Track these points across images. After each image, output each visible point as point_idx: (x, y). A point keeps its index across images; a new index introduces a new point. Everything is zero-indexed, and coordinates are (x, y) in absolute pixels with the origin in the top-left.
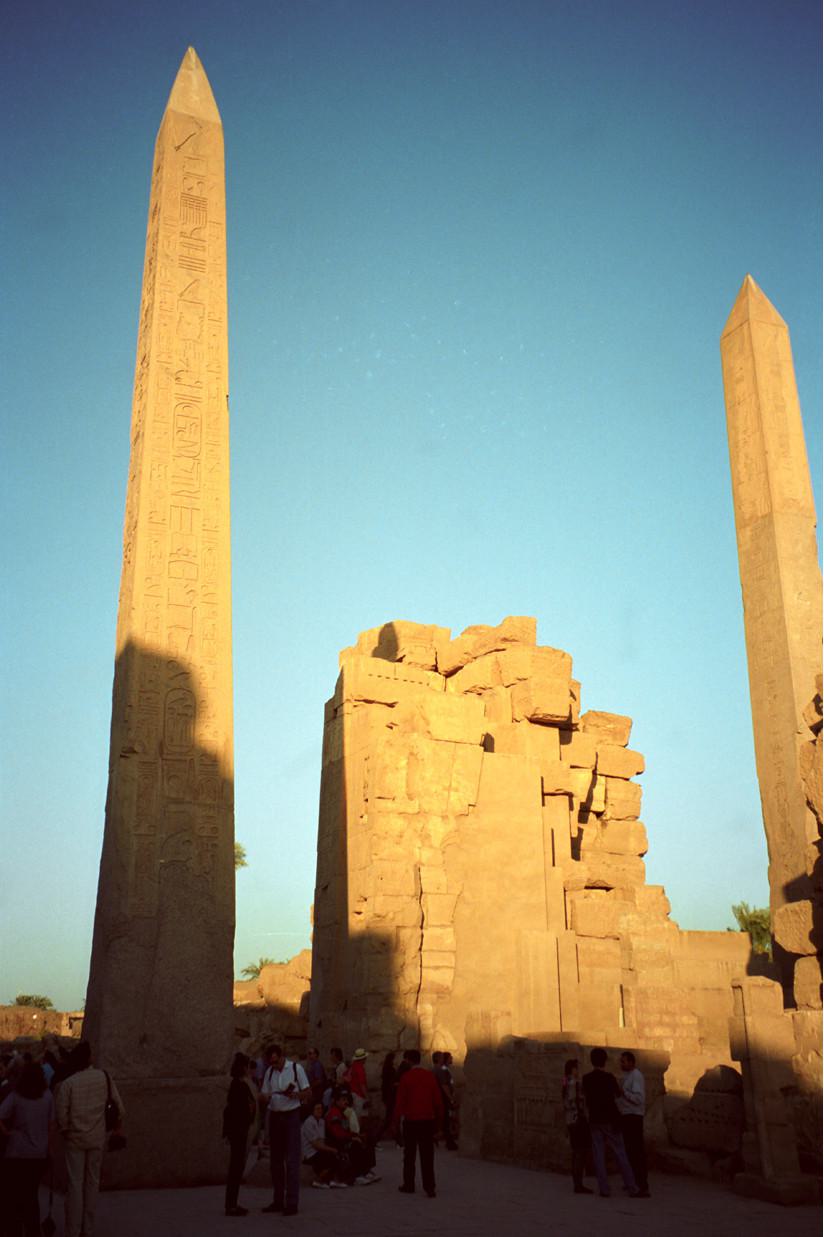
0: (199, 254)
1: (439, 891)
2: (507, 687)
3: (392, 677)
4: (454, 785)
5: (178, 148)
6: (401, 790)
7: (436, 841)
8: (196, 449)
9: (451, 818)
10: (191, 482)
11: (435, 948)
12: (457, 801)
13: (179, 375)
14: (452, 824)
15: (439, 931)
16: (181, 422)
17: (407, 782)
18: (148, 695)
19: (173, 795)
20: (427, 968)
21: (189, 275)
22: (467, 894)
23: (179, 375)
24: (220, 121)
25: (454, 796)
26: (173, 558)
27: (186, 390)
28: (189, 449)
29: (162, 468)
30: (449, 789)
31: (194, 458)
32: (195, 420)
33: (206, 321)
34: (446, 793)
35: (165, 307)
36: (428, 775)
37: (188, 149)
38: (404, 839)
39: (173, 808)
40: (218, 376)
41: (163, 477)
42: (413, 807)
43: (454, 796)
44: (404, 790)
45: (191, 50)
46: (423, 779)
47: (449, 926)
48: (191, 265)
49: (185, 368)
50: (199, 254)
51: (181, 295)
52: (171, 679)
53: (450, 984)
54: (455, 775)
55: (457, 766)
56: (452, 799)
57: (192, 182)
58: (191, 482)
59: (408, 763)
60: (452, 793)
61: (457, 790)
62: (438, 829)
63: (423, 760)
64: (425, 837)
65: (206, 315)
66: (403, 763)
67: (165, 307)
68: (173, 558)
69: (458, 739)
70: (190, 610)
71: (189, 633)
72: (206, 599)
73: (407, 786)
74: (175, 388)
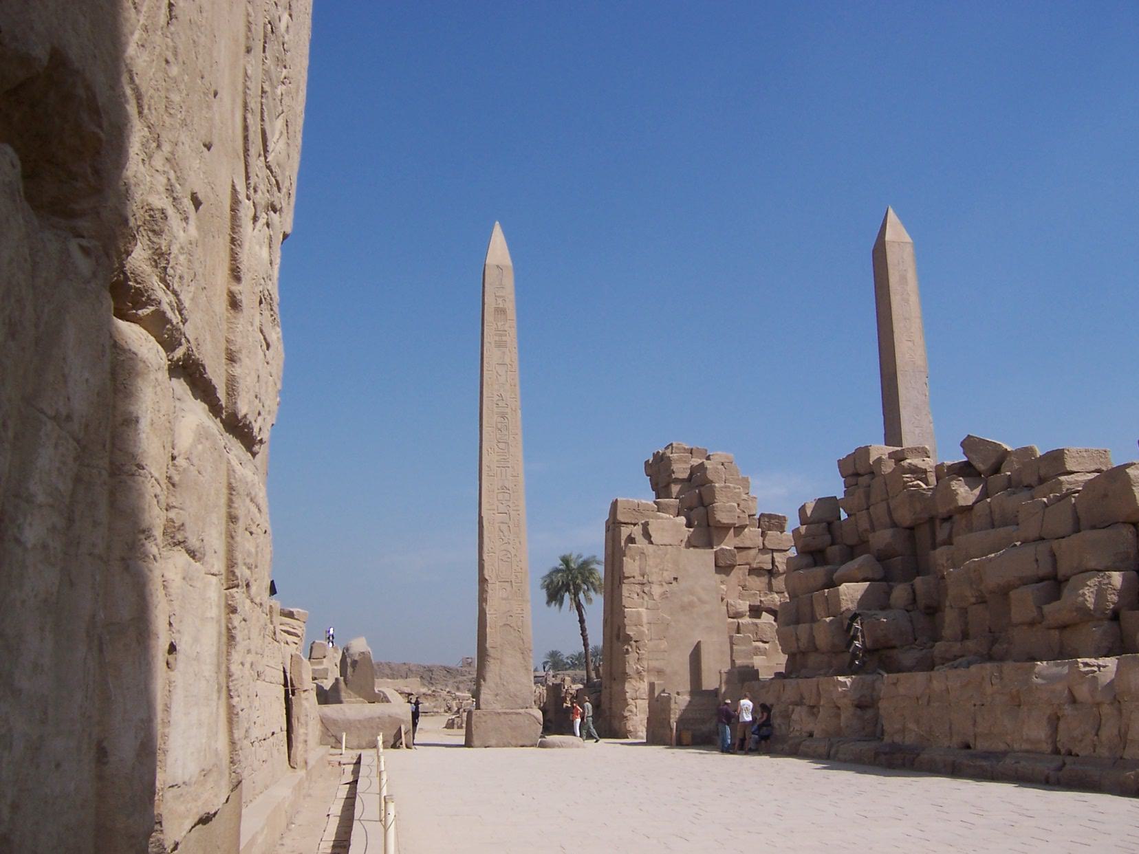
0: (504, 338)
3: (637, 509)
4: (665, 568)
6: (637, 574)
9: (664, 583)
12: (668, 576)
17: (640, 568)
22: (673, 623)
23: (498, 403)
24: (511, 264)
30: (662, 570)
31: (506, 443)
34: (661, 572)
39: (504, 601)
43: (665, 574)
44: (638, 572)
45: (497, 223)
48: (501, 345)
50: (504, 338)
55: (668, 556)
56: (664, 575)
59: (640, 559)
60: (664, 572)
61: (667, 570)
66: (637, 558)
72: (515, 508)
74: (496, 410)
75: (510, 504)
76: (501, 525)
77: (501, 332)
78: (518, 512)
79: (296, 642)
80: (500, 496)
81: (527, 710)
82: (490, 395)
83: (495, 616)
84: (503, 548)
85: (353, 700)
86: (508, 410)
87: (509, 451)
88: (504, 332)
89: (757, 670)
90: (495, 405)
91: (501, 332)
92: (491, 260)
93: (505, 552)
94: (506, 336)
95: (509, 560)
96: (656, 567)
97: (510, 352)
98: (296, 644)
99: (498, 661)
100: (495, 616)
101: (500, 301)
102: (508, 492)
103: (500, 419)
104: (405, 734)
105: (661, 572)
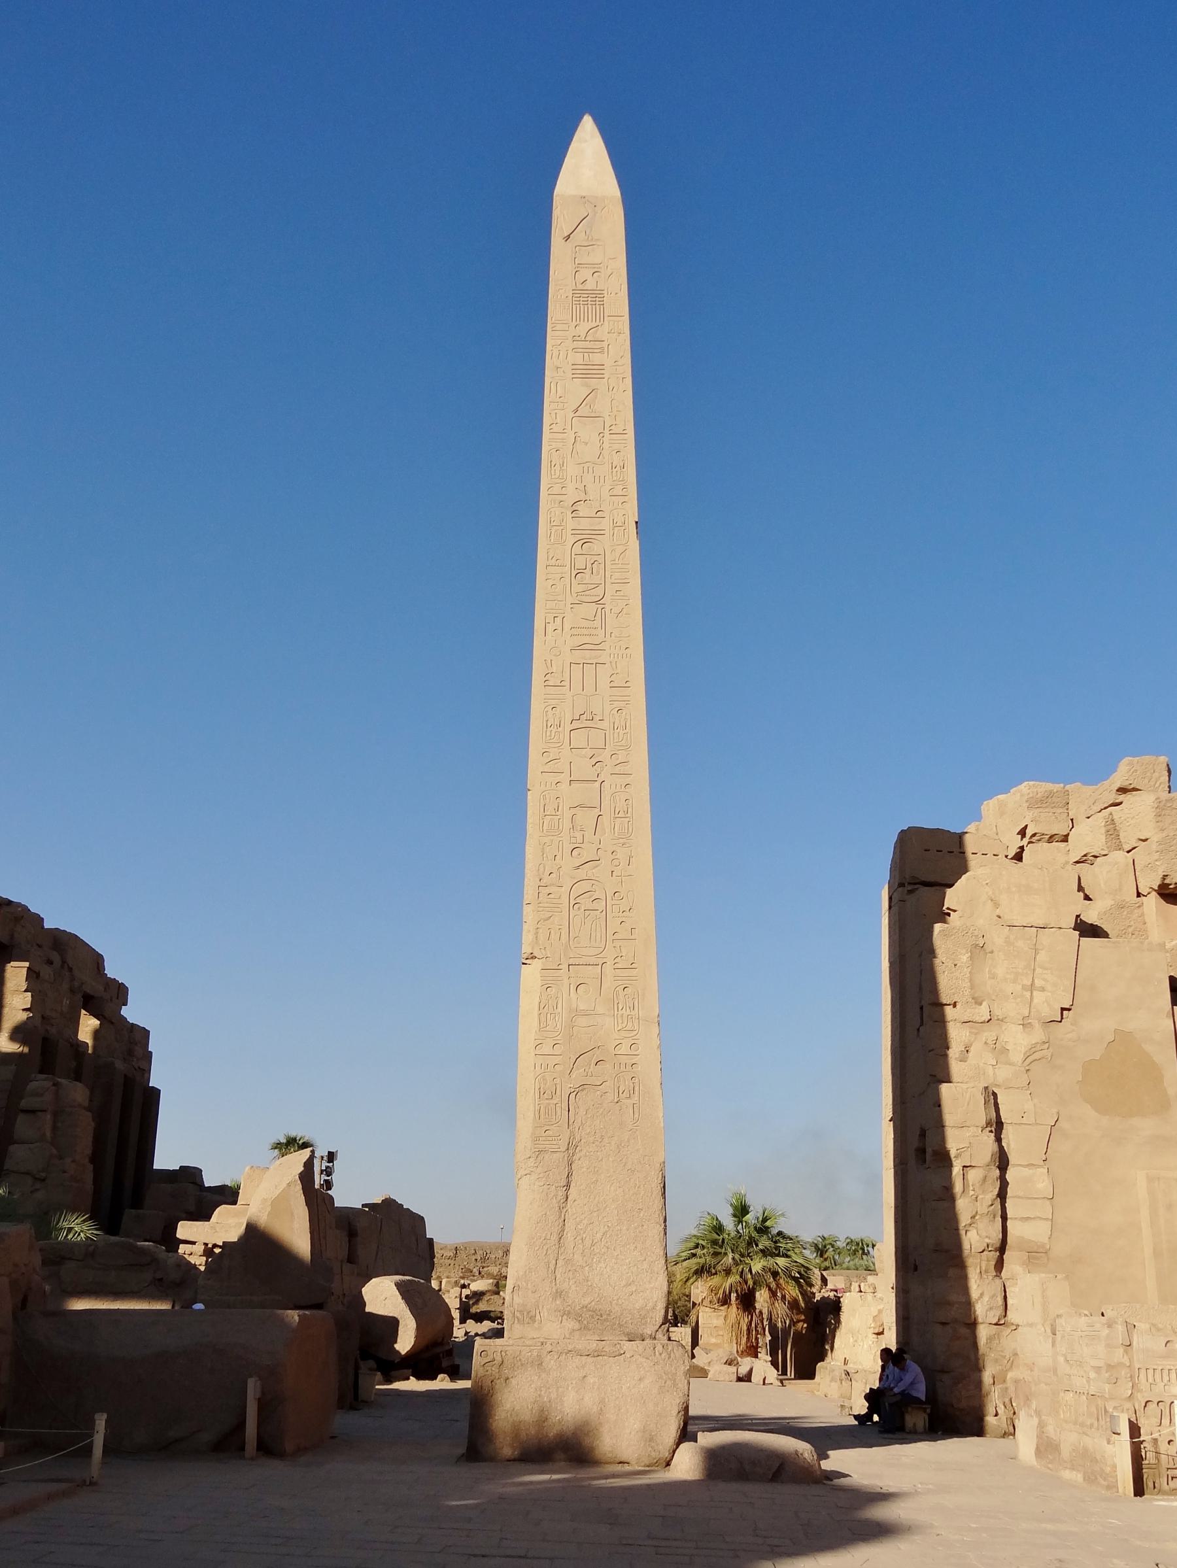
0: (597, 358)
1: (1024, 1121)
2: (1128, 852)
4: (1038, 983)
7: (1017, 1057)
8: (599, 591)
9: (1037, 1025)
10: (593, 632)
11: (1021, 1194)
12: (1046, 1004)
13: (574, 508)
14: (1038, 1034)
15: (1027, 1172)
17: (971, 980)
19: (582, 1007)
20: (1047, 1219)
25: (1039, 997)
26: (576, 725)
27: (584, 524)
29: (558, 620)
32: (596, 558)
35: (556, 428)
36: (1000, 971)
37: (579, 236)
38: (970, 1054)
40: (622, 499)
41: (559, 631)
42: (982, 1013)
46: (993, 977)
47: (1040, 1166)
49: (583, 497)
52: (578, 868)
53: (1046, 1240)
54: (1038, 970)
55: (1042, 956)
56: (1035, 1001)
57: (585, 273)
58: (593, 632)
59: (971, 958)
60: (1035, 993)
61: (1043, 989)
62: (1018, 1040)
63: (992, 952)
64: (999, 1050)
65: (607, 431)
66: (965, 958)
67: (556, 428)
68: (576, 725)
69: (1041, 923)
70: (597, 784)
71: (596, 812)
72: (617, 770)
73: (972, 987)
74: (570, 524)
75: (605, 756)
78: (628, 780)
80: (579, 738)
82: (556, 489)
84: (581, 874)
86: (605, 524)
87: (604, 624)
90: (570, 515)
92: (566, 186)
94: (602, 352)
95: (595, 905)
96: (1015, 981)
105: (1028, 994)
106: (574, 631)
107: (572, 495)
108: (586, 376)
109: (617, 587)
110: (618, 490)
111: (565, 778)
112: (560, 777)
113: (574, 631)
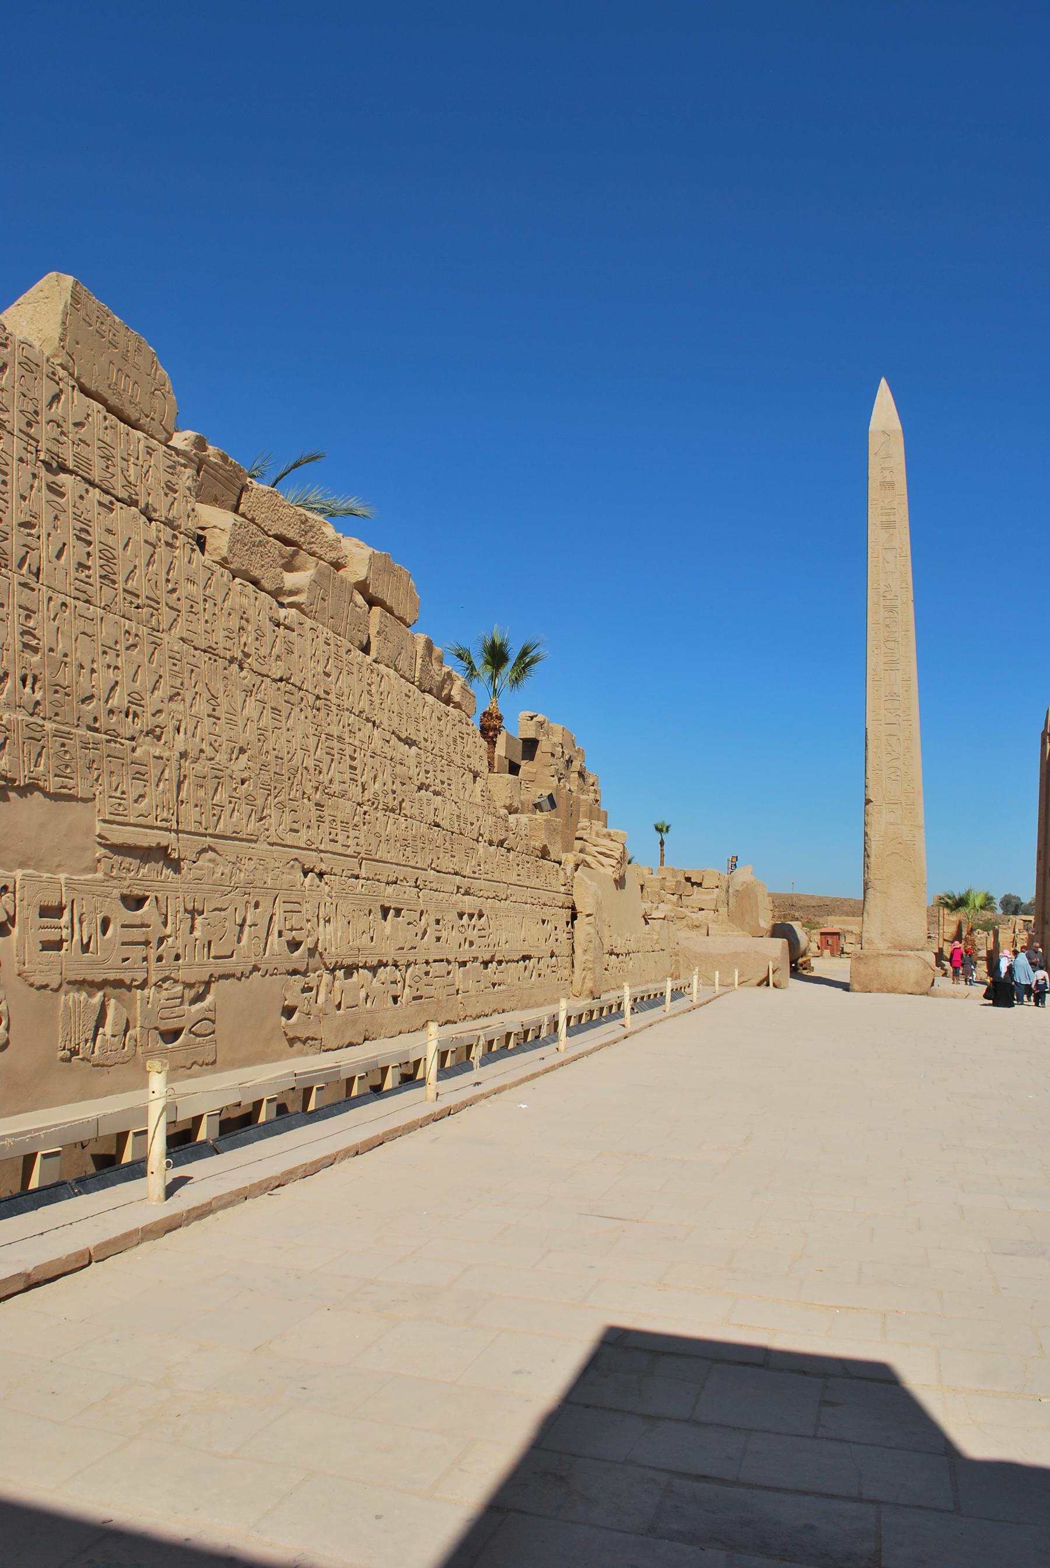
0: (892, 518)
5: (876, 454)
8: (896, 635)
10: (894, 655)
16: (887, 622)
18: (876, 772)
19: (892, 821)
21: (886, 532)
27: (888, 603)
28: (892, 636)
33: (898, 558)
39: (892, 827)
45: (883, 381)
48: (889, 526)
51: (882, 546)
58: (894, 655)
72: (905, 718)
74: (882, 603)
75: (899, 712)
76: (889, 737)
77: (889, 511)
78: (910, 723)
79: (614, 865)
81: (920, 953)
83: (881, 842)
85: (735, 933)
88: (893, 511)
89: (22, 798)
90: (882, 598)
91: (889, 511)
93: (893, 770)
97: (900, 534)
98: (614, 867)
99: (884, 895)
100: (881, 842)
101: (886, 473)
102: (898, 698)
103: (887, 615)
104: (774, 972)
106: (885, 655)
107: (883, 589)
108: (887, 528)
109: (904, 633)
110: (904, 586)
111: (882, 723)
112: (880, 722)
113: (885, 655)
